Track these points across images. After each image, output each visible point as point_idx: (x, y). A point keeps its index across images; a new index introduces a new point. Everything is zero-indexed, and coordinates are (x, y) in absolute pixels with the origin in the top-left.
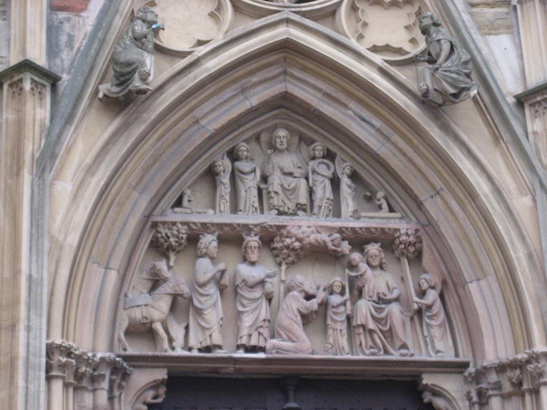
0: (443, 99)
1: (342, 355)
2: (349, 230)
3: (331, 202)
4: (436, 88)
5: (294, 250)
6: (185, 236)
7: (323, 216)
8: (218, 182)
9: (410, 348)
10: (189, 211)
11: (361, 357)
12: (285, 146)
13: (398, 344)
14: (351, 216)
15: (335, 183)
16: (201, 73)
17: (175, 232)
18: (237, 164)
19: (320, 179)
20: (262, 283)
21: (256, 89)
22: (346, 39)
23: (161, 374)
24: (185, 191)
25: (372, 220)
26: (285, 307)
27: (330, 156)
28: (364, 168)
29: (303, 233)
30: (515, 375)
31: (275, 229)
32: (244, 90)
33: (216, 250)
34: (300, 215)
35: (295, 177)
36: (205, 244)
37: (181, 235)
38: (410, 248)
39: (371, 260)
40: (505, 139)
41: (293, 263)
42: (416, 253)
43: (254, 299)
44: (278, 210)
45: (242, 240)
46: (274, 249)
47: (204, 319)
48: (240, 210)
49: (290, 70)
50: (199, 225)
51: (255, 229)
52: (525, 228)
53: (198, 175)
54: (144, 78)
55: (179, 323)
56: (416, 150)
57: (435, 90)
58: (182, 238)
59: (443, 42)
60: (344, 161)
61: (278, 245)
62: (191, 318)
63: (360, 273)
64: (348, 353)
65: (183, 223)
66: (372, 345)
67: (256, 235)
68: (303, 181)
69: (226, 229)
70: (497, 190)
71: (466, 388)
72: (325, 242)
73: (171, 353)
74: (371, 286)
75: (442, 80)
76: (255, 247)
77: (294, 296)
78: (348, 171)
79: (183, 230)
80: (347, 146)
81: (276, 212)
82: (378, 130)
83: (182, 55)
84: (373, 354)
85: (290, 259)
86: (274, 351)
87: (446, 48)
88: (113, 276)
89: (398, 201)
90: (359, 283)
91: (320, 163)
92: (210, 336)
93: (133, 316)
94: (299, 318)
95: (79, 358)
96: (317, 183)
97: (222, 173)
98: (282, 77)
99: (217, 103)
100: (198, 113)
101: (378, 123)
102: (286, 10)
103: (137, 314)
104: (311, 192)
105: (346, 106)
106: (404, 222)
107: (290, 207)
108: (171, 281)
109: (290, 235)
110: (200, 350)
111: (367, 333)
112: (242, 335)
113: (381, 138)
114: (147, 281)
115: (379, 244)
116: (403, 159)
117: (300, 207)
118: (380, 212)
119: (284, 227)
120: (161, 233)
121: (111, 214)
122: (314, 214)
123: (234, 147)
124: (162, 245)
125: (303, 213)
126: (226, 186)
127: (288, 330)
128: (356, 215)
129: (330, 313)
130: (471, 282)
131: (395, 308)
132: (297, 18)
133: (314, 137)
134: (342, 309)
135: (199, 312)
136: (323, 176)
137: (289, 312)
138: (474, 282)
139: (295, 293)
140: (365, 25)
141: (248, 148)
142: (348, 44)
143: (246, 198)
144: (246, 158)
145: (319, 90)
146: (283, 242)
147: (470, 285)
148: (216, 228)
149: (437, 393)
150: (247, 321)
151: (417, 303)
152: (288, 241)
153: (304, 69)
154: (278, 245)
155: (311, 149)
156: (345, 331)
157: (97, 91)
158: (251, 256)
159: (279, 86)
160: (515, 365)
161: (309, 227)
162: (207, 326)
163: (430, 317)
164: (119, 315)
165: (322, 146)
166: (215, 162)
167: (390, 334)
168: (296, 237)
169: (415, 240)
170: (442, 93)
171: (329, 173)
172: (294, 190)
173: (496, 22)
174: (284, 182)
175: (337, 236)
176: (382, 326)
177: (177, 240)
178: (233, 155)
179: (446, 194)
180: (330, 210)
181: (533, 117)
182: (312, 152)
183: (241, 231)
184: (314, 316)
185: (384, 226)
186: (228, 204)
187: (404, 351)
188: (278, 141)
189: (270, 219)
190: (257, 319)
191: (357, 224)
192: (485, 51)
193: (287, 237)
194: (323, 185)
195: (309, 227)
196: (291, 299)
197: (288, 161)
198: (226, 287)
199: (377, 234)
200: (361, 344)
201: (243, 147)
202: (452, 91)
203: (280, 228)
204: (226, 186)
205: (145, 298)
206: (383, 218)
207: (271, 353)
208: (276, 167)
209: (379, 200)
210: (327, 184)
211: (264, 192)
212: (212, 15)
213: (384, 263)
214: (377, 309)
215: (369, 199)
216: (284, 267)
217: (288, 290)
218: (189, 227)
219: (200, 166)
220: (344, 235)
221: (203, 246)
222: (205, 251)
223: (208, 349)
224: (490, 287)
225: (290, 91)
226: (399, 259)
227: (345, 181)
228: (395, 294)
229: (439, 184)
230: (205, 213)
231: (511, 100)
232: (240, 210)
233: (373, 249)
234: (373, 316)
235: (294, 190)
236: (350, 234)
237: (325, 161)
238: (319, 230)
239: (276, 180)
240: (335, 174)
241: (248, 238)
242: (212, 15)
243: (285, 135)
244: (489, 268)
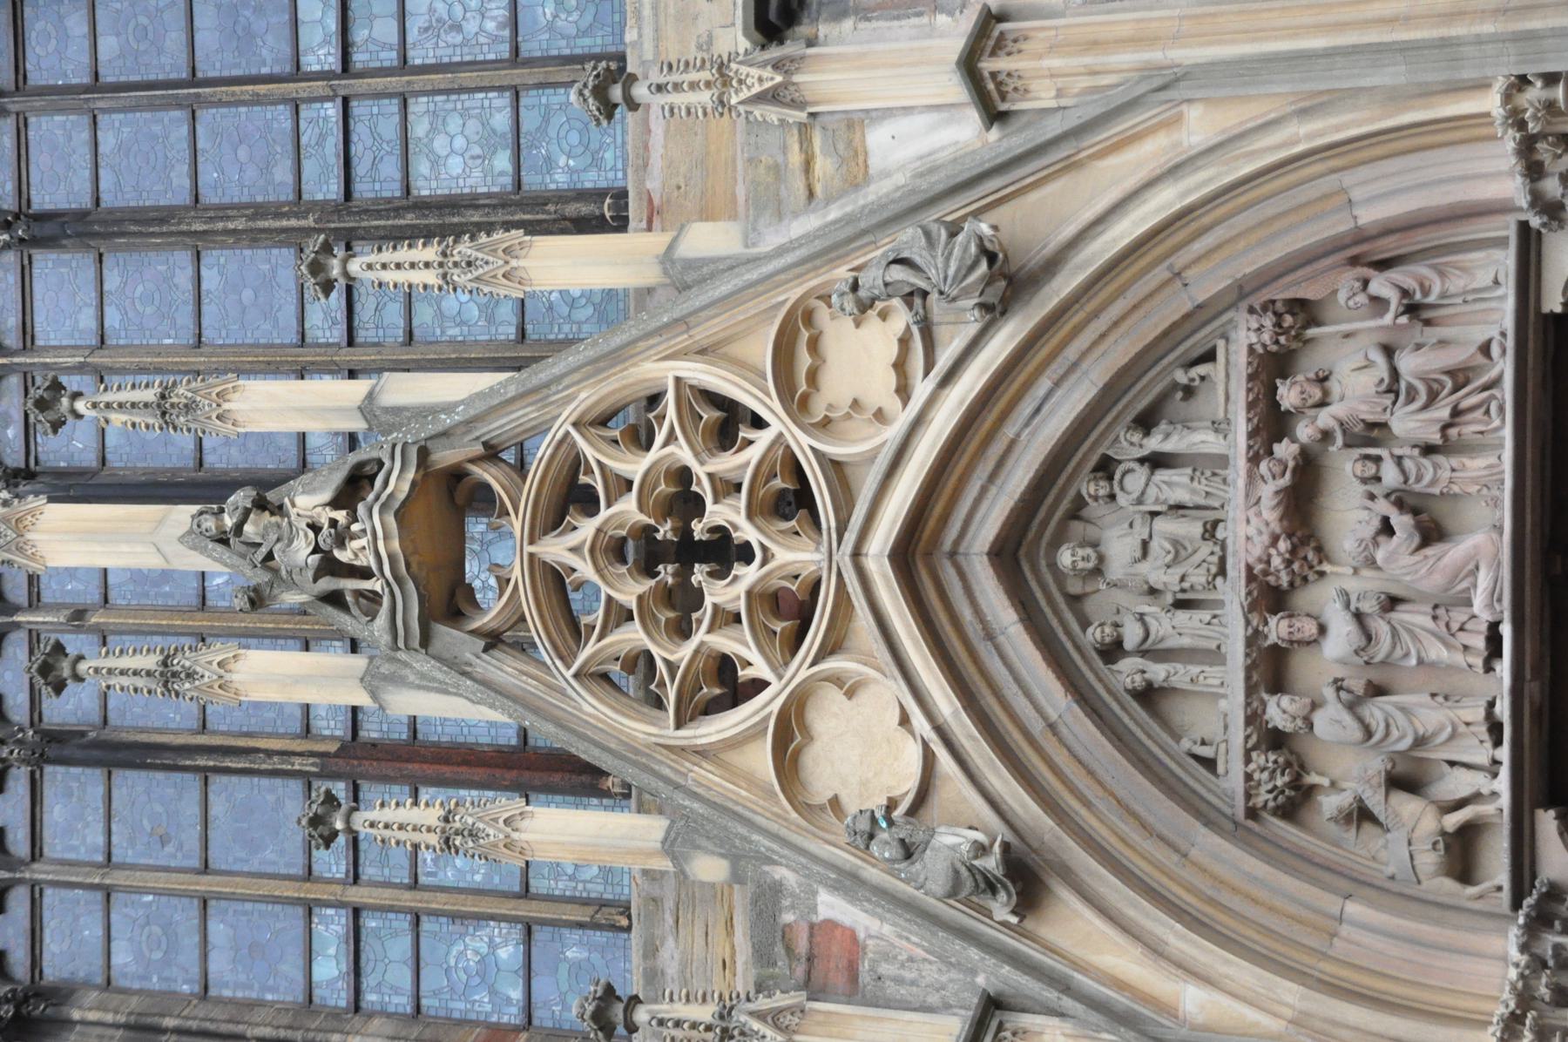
0: (999, 280)
1: (1503, 472)
2: (1251, 443)
3: (1198, 473)
4: (978, 294)
5: (1293, 551)
6: (1272, 757)
7: (1226, 492)
8: (1165, 685)
9: (1486, 337)
10: (1223, 747)
11: (1508, 433)
12: (1089, 551)
13: (1481, 360)
14: (1225, 437)
15: (1157, 461)
16: (964, 726)
17: (1265, 775)
18: (1130, 643)
19: (1152, 492)
20: (1359, 617)
21: (985, 610)
22: (885, 449)
23: (1547, 821)
24: (1185, 749)
25: (1232, 397)
26: (1408, 578)
27: (1106, 467)
28: (1130, 402)
29: (1260, 533)
30: (1547, 151)
31: (1254, 585)
32: (990, 636)
33: (1297, 698)
34: (1224, 535)
35: (1151, 536)
36: (1286, 720)
37: (1270, 765)
38: (1286, 325)
39: (1310, 402)
40: (1072, 152)
41: (1319, 549)
42: (1297, 310)
43: (1393, 636)
44: (1215, 577)
45: (1275, 647)
46: (1291, 584)
47: (1435, 734)
48: (1219, 647)
49: (947, 545)
50: (1249, 730)
51: (1255, 623)
52: (1251, 119)
53: (1150, 721)
54: (981, 850)
55: (1442, 777)
56: (1096, 314)
57: (981, 294)
58: (1275, 762)
59: (888, 279)
60: (1117, 439)
61: (1284, 580)
62: (1432, 756)
63: (1337, 428)
64: (1499, 458)
65: (1248, 760)
66: (1482, 410)
67: (1266, 623)
68: (1161, 525)
69: (1255, 677)
70: (1174, 171)
72: (1277, 493)
73: (1505, 801)
74: (1364, 407)
75: (964, 284)
76: (1290, 627)
77: (1387, 560)
78: (1136, 437)
79: (1259, 758)
80: (1087, 436)
81: (1219, 580)
82: (1057, 384)
83: (929, 759)
84: (1501, 409)
85: (1311, 555)
86: (1496, 605)
87: (898, 273)
88: (1353, 909)
89: (1195, 344)
90: (1359, 428)
91: (1122, 489)
92: (1468, 724)
93: (1432, 868)
94: (1429, 551)
95: (1525, 998)
96: (1162, 497)
97: (1146, 676)
98: (961, 559)
99: (1014, 688)
100: (1037, 726)
101: (1044, 385)
102: (835, 558)
103: (1429, 860)
104: (1179, 507)
105: (1012, 443)
106: (1233, 335)
107: (1209, 551)
108: (1360, 791)
109: (1265, 558)
110: (1498, 743)
111: (1457, 420)
112: (1465, 664)
113: (1073, 378)
114: (1361, 831)
115: (1278, 382)
116: (1111, 338)
117: (1210, 531)
118: (1215, 379)
119: (1249, 568)
120: (1266, 802)
121: (1236, 903)
122: (1222, 506)
123: (1096, 649)
124: (1289, 798)
125: (1221, 525)
126: (1172, 671)
127: (1454, 578)
128: (1220, 427)
129: (1418, 488)
130: (1355, 218)
131: (1408, 363)
132: (850, 537)
133: (1072, 493)
134: (1408, 464)
136: (1147, 485)
137: (1416, 572)
138: (1355, 212)
139: (1380, 556)
140: (856, 404)
141: (1096, 624)
142: (898, 441)
143: (1193, 636)
144: (1116, 625)
145: (984, 491)
146: (1278, 571)
147: (1361, 222)
148: (1255, 697)
150: (1437, 652)
151: (1396, 317)
152: (1277, 562)
153: (945, 519)
154: (1284, 580)
155: (1095, 504)
156: (1454, 461)
157: (1005, 924)
158: (1307, 634)
159: (979, 567)
160: (1527, 147)
161: (1248, 521)
162: (1449, 729)
163: (1426, 293)
164: (1431, 897)
165: (1089, 481)
166: (1127, 690)
167: (1460, 377)
168: (1267, 547)
169: (1270, 314)
170: (989, 281)
171: (1142, 473)
172: (1177, 543)
173: (841, 153)
174: (1159, 563)
175: (1264, 467)
176: (1444, 388)
177: (1278, 772)
178: (1112, 651)
179: (1180, 260)
180: (1214, 474)
181: (1029, 96)
182: (1101, 501)
183: (1259, 649)
184: (1424, 517)
185: (1244, 375)
186: (1207, 668)
187: (1495, 350)
188: (1081, 565)
189: (1233, 594)
190: (1434, 634)
191: (1241, 427)
192: (900, 179)
193: (1268, 562)
194: (1164, 487)
195: (1248, 521)
196: (1393, 566)
197: (1120, 547)
198: (1369, 683)
199: (1258, 387)
200: (1482, 433)
201: (1094, 635)
202: (983, 267)
203: (1251, 576)
204: (1172, 671)
205: (1397, 837)
206: (1227, 375)
207: (1502, 612)
208: (1132, 570)
209: (1193, 380)
210: (1166, 478)
211: (1180, 596)
212: (850, 694)
213: (1317, 374)
214: (1411, 399)
215: (1189, 391)
216: (1326, 567)
217: (1371, 563)
218: (1254, 748)
219: (1135, 718)
220: (1261, 452)
221: (1288, 725)
222: (1299, 722)
223: (1495, 729)
224: (1365, 183)
225: (986, 548)
226: (1307, 342)
227: (1154, 443)
228: (1379, 358)
229: (1160, 273)
230: (1226, 715)
231: (994, 134)
232: (1219, 647)
233: (1288, 395)
234: (1425, 407)
235: (1177, 543)
236: (1259, 439)
237: (1117, 477)
238: (1253, 501)
239: (1155, 572)
240: (1142, 461)
241: (1273, 638)
242: (850, 694)
243: (1069, 552)
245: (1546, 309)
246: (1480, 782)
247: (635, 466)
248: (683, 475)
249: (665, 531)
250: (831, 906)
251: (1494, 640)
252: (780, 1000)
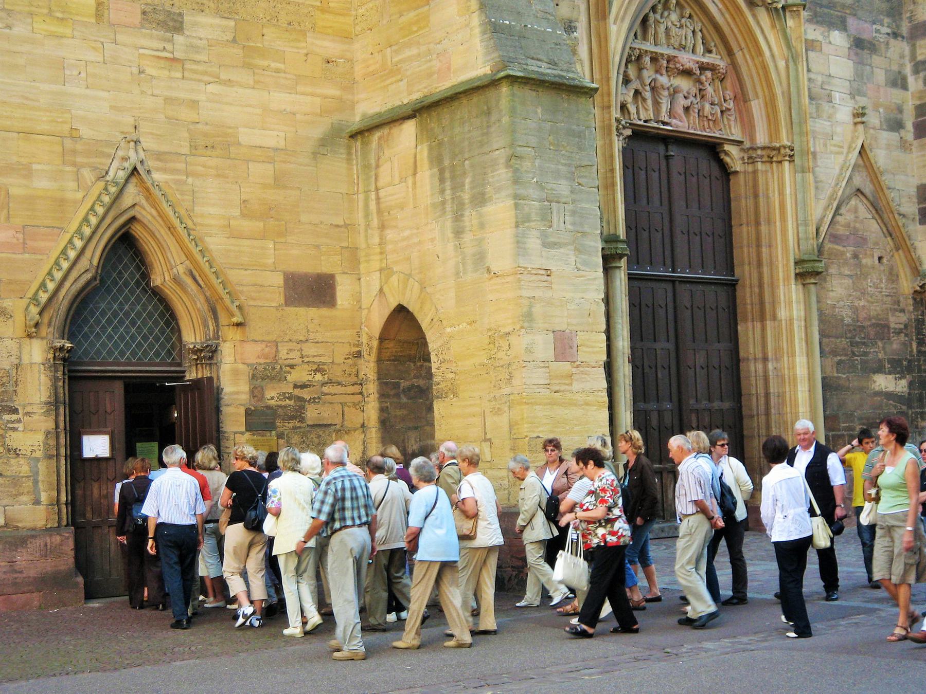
11: (705, 134)
15: (694, 32)
70: (773, 56)
71: (742, 155)
90: (704, 93)
110: (645, 121)
135: (644, 100)
149: (727, 154)
179: (745, 51)
229: (743, 45)
244: (760, 94)
245: (725, 145)
251: (664, 123)
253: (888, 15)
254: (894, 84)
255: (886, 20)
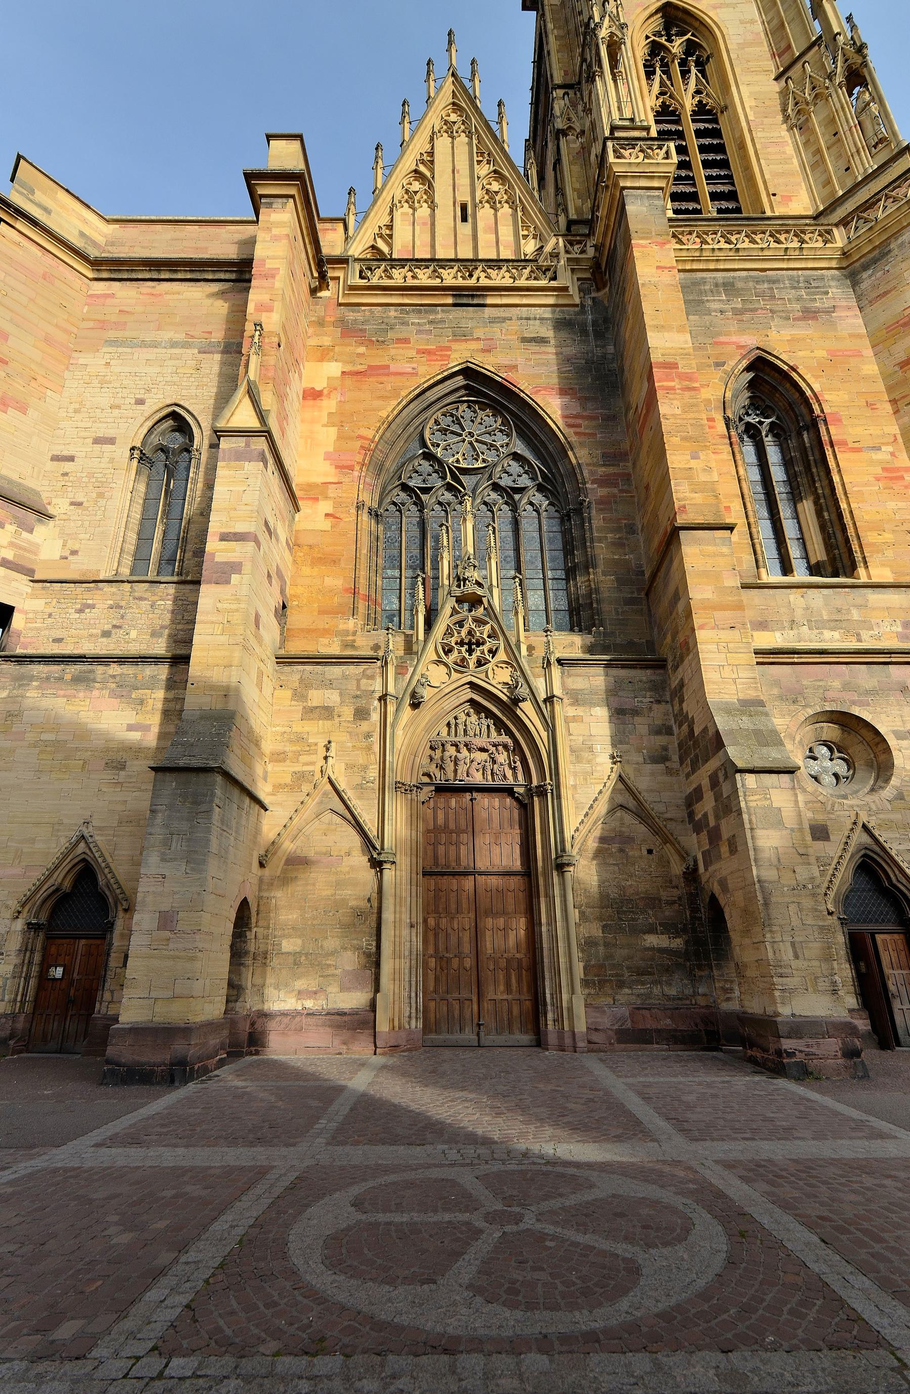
23: (433, 788)
160: (541, 786)
167: (505, 776)
189: (467, 739)
246: (438, 778)
247: (485, 636)
248: (483, 644)
249: (474, 641)
250: (411, 670)
252: (395, 661)
253: (650, 690)
254: (658, 732)
255: (648, 694)
